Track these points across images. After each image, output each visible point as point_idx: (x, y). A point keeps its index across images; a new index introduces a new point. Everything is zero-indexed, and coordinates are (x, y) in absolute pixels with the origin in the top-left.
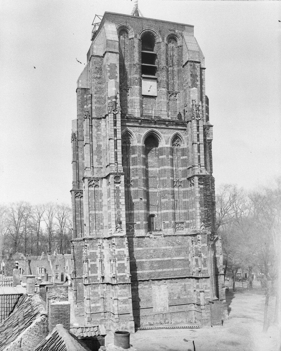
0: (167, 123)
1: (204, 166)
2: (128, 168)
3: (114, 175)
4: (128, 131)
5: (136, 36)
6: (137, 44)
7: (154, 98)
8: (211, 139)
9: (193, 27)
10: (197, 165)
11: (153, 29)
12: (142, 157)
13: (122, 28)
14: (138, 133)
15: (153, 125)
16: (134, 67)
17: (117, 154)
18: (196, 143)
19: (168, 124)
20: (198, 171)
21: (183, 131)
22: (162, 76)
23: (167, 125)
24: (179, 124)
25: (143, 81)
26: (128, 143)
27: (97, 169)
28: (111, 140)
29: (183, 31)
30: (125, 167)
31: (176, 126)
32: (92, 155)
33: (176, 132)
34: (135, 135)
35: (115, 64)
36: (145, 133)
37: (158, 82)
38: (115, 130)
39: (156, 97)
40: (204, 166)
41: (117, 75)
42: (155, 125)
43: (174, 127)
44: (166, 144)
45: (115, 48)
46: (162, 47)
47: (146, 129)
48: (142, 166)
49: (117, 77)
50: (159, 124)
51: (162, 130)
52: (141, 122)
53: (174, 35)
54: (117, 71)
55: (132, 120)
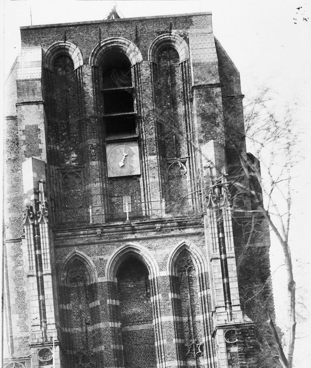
0: (158, 226)
1: (238, 305)
2: (84, 331)
3: (37, 348)
4: (76, 255)
5: (86, 62)
6: (89, 78)
7: (136, 179)
8: (267, 245)
9: (211, 15)
10: (223, 304)
11: (122, 40)
12: (109, 305)
13: (59, 52)
14: (97, 258)
15: (129, 235)
16: (87, 125)
17: (44, 305)
18: (217, 258)
19: (162, 227)
20: (226, 318)
21: (196, 238)
22: (149, 132)
23: (160, 230)
24: (185, 225)
25: (109, 149)
26: (81, 281)
27: (20, 341)
28: (31, 278)
29: (188, 28)
30: (77, 329)
31: (180, 229)
32: (10, 314)
33: (180, 241)
34: (92, 262)
35: (36, 126)
36: (113, 254)
37: (140, 146)
38: (39, 258)
39: (139, 176)
40: (238, 305)
41: (40, 146)
42: (133, 233)
43: (177, 232)
44: (161, 270)
45: (34, 94)
46: (144, 70)
47: (115, 247)
48: (110, 323)
49: (40, 151)
50: (142, 231)
51: (150, 242)
52: (103, 232)
53: (170, 41)
54: (41, 138)
55: (82, 232)
